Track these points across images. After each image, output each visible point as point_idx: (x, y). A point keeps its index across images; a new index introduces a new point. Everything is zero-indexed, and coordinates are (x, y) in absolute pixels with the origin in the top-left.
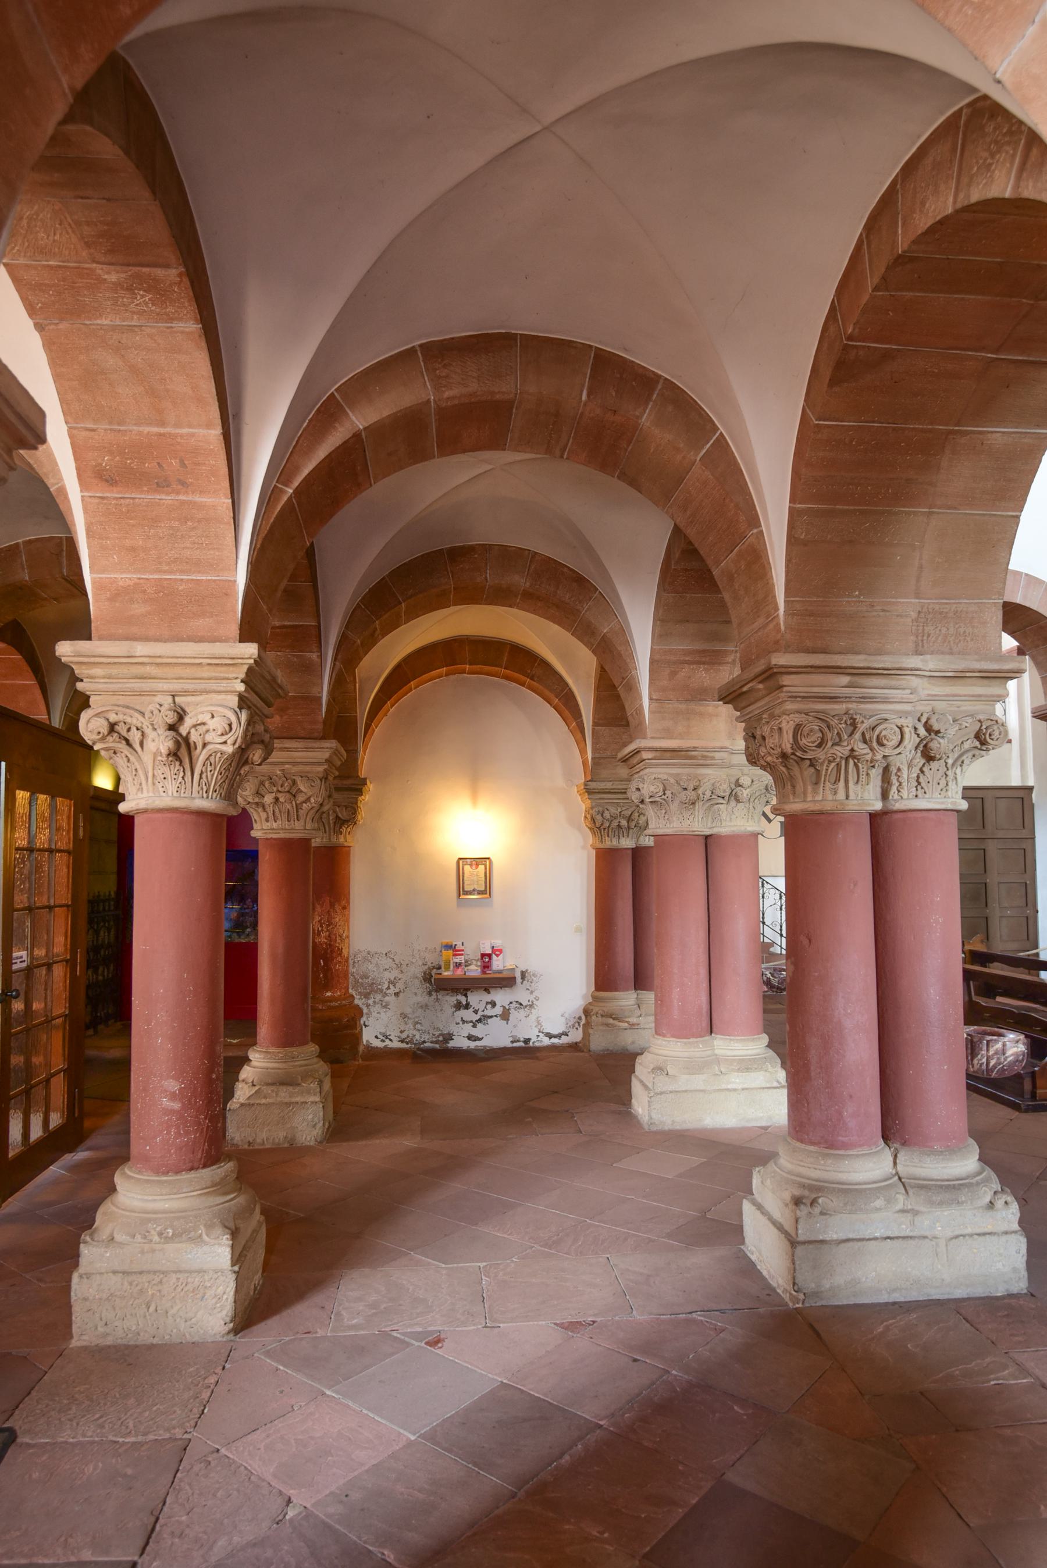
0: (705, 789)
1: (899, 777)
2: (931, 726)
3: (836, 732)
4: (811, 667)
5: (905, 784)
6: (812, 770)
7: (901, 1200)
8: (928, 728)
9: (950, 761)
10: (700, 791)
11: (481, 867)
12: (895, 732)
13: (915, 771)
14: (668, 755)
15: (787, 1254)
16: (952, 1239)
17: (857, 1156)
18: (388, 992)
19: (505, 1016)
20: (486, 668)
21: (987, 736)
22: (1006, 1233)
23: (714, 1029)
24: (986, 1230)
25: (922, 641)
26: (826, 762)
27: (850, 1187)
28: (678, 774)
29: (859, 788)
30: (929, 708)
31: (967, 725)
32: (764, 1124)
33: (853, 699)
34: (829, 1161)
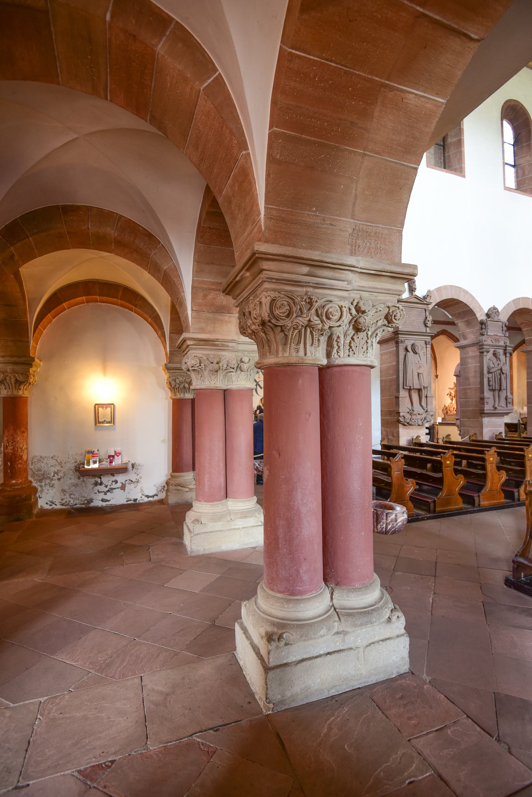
0: (223, 364)
1: (338, 342)
2: (360, 308)
3: (299, 307)
4: (283, 256)
5: (342, 347)
6: (282, 335)
7: (336, 626)
8: (358, 309)
9: (370, 333)
10: (221, 365)
11: (109, 409)
12: (337, 310)
13: (349, 339)
14: (202, 343)
15: (262, 675)
16: (367, 646)
17: (309, 599)
18: (54, 478)
19: (123, 487)
20: (110, 299)
21: (393, 317)
22: (398, 636)
23: (228, 496)
24: (387, 637)
25: (355, 250)
26: (292, 329)
27: (305, 622)
28: (208, 355)
29: (313, 348)
30: (358, 296)
31: (381, 309)
32: (254, 545)
33: (311, 284)
34: (291, 605)
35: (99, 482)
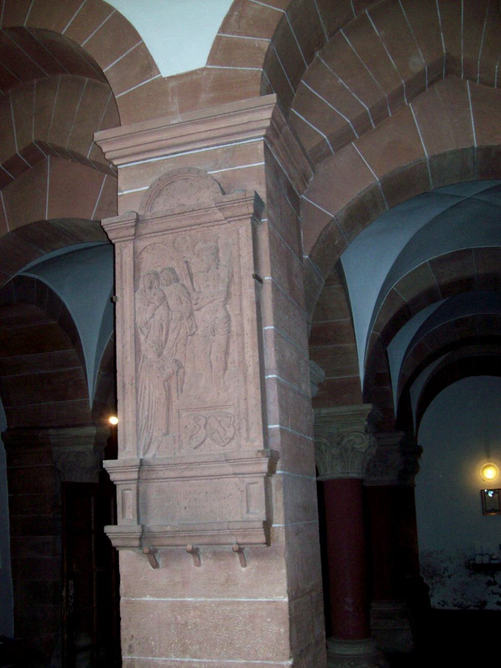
18: (444, 575)
35: (493, 581)
